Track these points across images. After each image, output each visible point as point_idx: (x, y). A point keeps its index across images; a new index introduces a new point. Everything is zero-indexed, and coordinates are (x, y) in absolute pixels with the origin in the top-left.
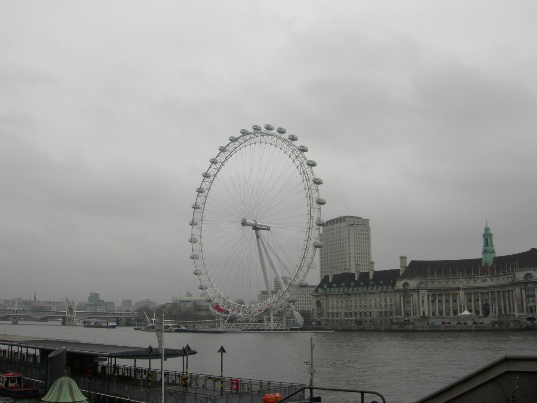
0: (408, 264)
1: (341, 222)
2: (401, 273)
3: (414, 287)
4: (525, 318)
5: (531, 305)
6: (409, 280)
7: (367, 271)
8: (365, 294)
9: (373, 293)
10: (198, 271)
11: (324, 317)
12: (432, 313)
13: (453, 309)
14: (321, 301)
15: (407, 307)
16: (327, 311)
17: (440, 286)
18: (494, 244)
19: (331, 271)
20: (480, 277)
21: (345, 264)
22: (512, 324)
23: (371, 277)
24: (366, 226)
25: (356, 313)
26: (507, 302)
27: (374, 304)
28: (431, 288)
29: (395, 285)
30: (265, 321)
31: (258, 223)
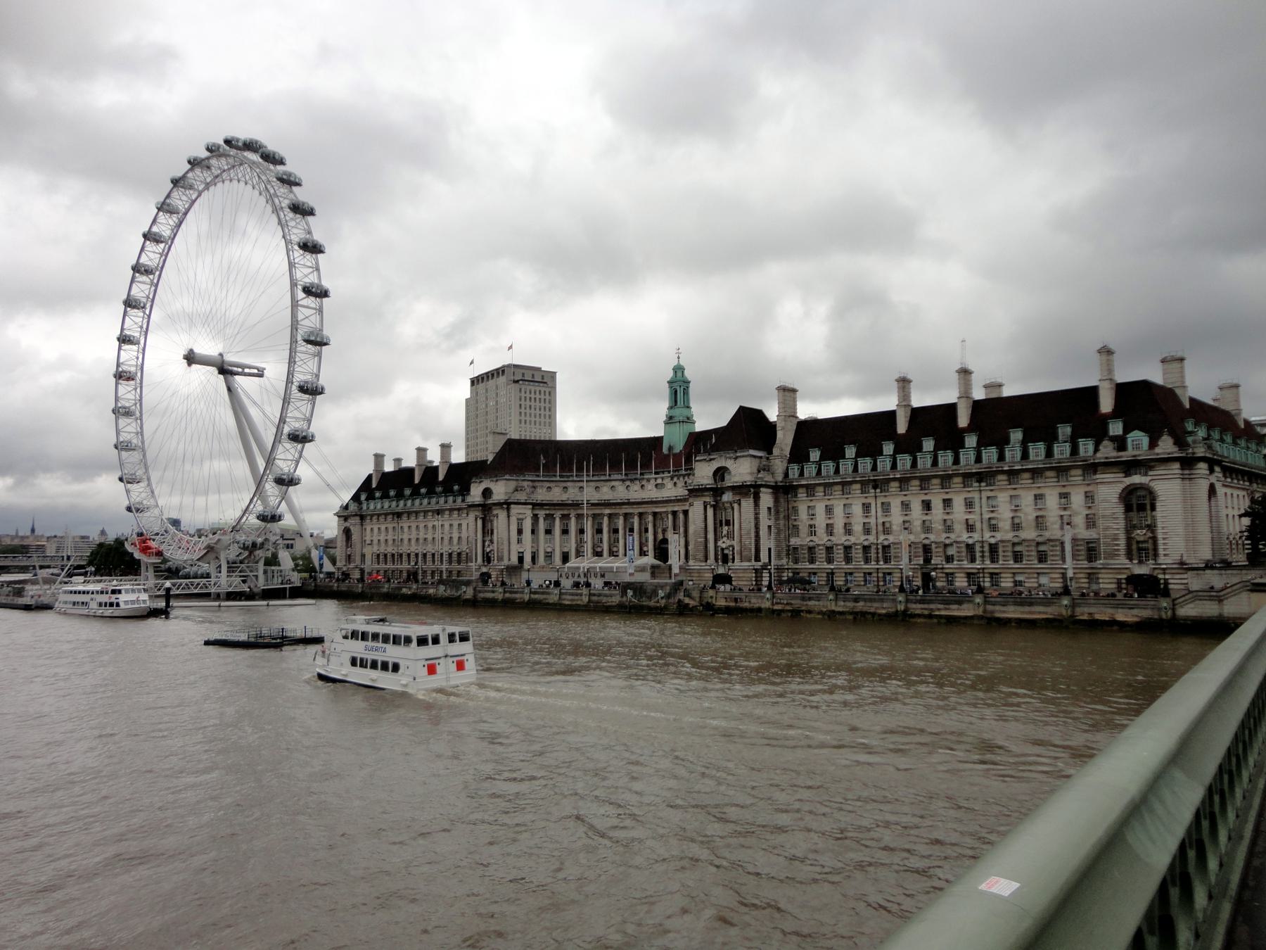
4: (709, 576)
5: (724, 546)
8: (426, 512)
9: (439, 512)
14: (352, 528)
15: (487, 544)
17: (564, 497)
18: (691, 405)
22: (660, 591)
23: (441, 478)
25: (409, 555)
27: (440, 537)
31: (229, 358)
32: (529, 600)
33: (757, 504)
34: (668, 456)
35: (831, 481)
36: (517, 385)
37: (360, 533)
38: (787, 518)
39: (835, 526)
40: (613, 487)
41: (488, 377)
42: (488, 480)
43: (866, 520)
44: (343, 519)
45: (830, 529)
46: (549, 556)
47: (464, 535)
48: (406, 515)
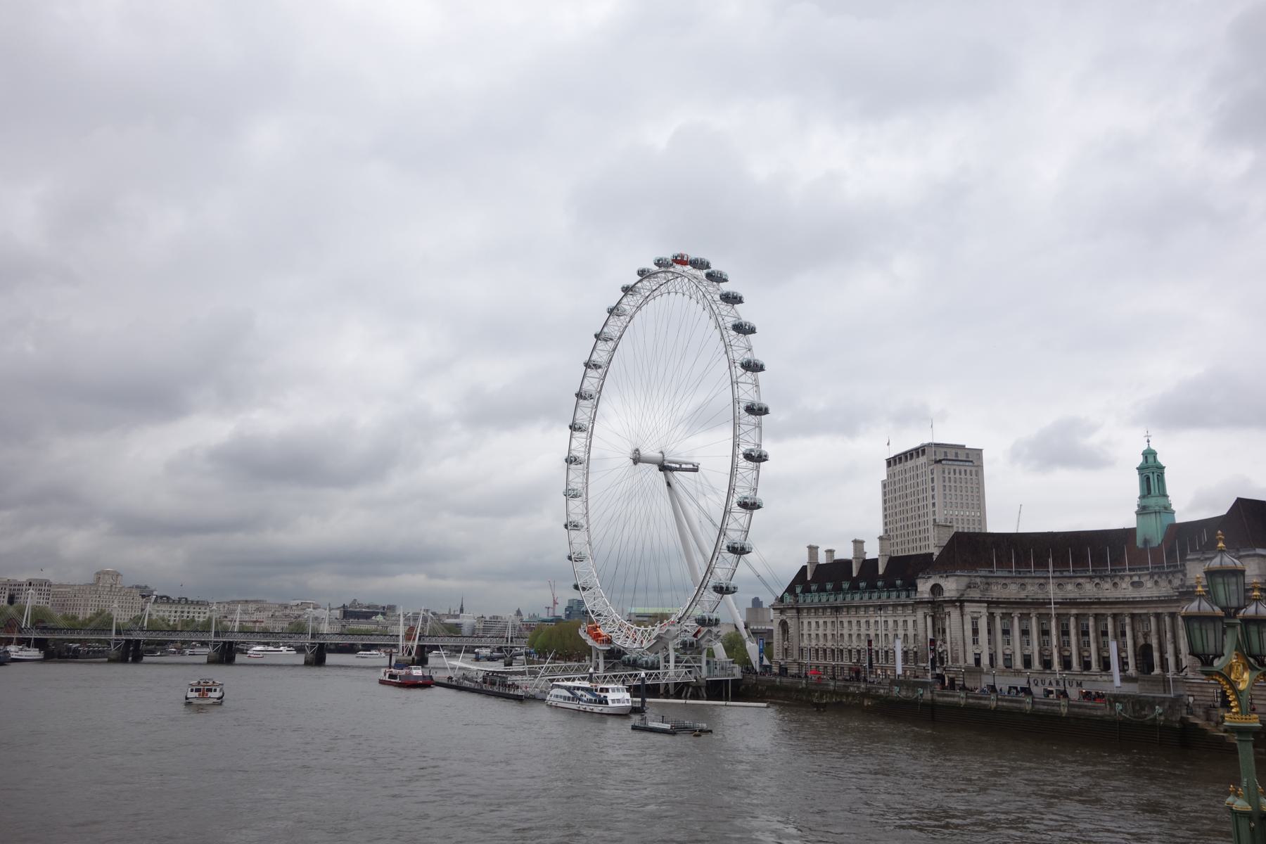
1: (918, 456)
6: (941, 577)
7: (906, 554)
8: (867, 607)
9: (880, 608)
11: (792, 657)
12: (1005, 660)
13: (1060, 652)
14: (787, 620)
17: (1023, 595)
18: (1168, 492)
20: (1126, 575)
21: (927, 543)
22: (1157, 707)
23: (881, 571)
24: (976, 464)
25: (850, 651)
27: (884, 633)
28: (998, 598)
29: (916, 590)
30: (662, 665)
31: (669, 457)
32: (996, 708)
34: (1144, 550)
36: (939, 465)
37: (797, 625)
40: (1079, 584)
41: (906, 457)
42: (938, 576)
44: (778, 611)
46: (1008, 660)
47: (911, 632)
48: (845, 610)
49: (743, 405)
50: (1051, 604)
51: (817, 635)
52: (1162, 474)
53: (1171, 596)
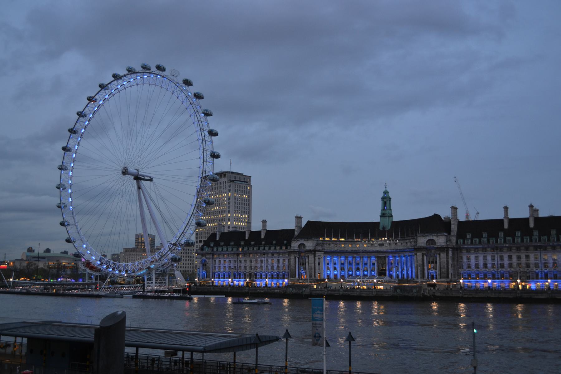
0: (303, 224)
2: (296, 233)
3: (310, 248)
6: (305, 240)
8: (256, 253)
9: (264, 254)
10: (66, 221)
14: (207, 260)
16: (213, 271)
17: (336, 249)
18: (392, 209)
19: (219, 229)
22: (414, 290)
23: (263, 237)
26: (405, 268)
31: (140, 173)
33: (447, 255)
35: (478, 246)
38: (458, 261)
39: (480, 265)
42: (303, 240)
43: (493, 263)
44: (201, 255)
45: (477, 266)
49: (208, 153)
50: (360, 253)
51: (225, 267)
52: (390, 201)
53: (397, 250)
